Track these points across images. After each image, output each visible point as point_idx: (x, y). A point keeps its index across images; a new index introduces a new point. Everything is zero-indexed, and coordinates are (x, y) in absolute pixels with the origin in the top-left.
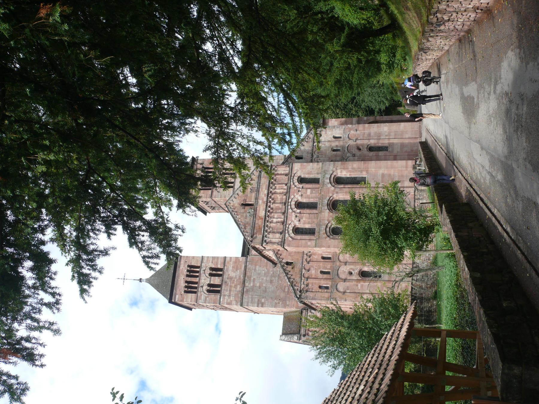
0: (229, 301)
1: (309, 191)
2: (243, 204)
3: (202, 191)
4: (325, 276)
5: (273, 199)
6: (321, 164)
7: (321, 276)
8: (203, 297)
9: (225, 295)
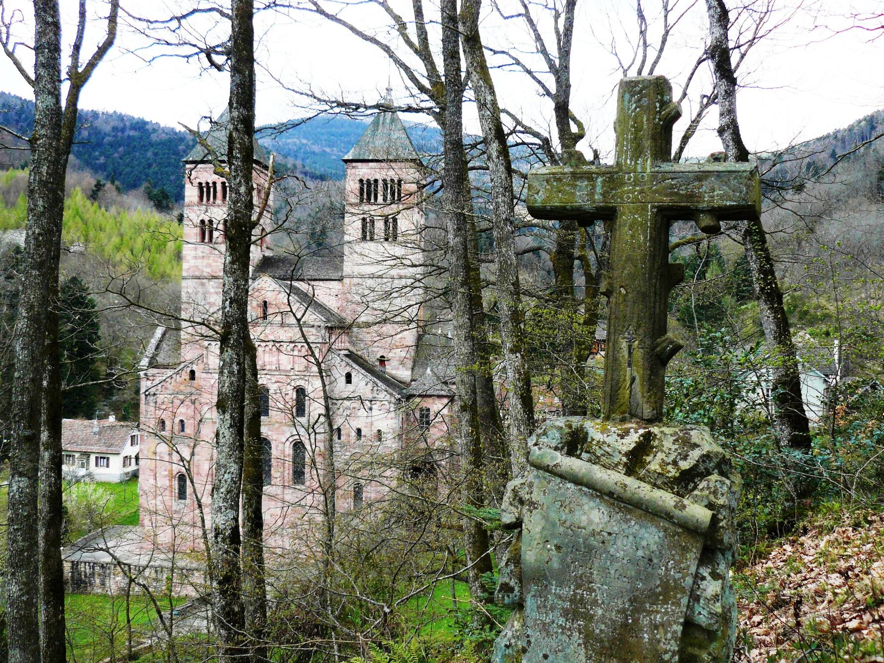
2: (265, 302)
3: (358, 186)
5: (271, 350)
7: (177, 420)
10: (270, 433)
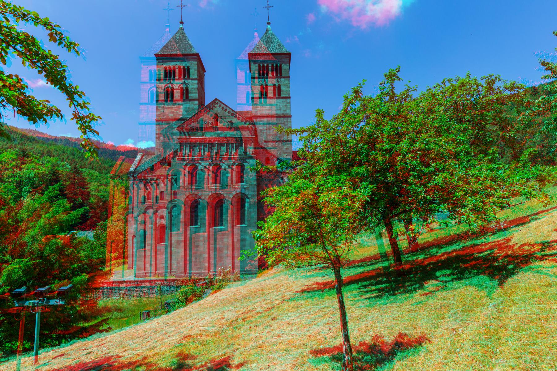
0: (159, 108)
1: (230, 175)
4: (159, 195)
6: (255, 183)
7: (159, 192)
8: (161, 85)
9: (164, 104)
10: (222, 193)
